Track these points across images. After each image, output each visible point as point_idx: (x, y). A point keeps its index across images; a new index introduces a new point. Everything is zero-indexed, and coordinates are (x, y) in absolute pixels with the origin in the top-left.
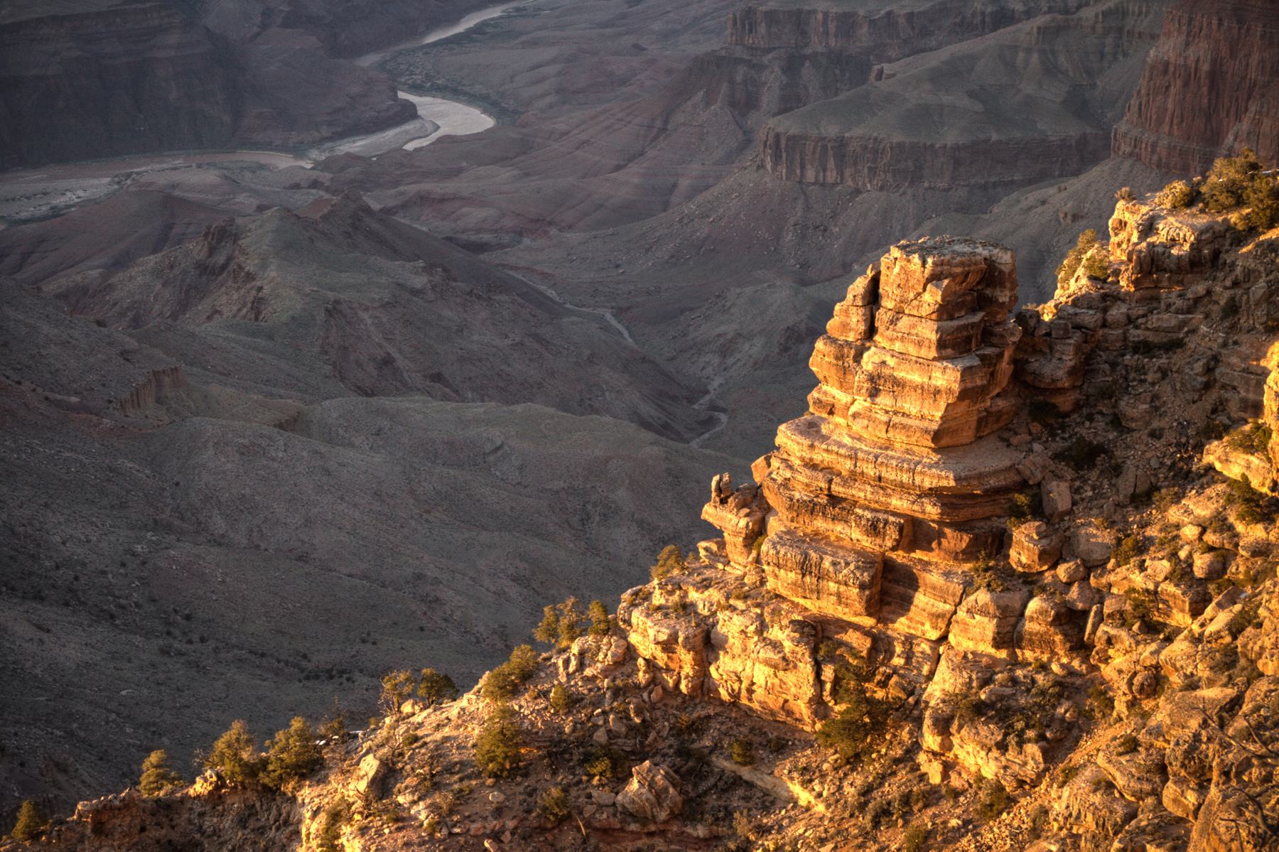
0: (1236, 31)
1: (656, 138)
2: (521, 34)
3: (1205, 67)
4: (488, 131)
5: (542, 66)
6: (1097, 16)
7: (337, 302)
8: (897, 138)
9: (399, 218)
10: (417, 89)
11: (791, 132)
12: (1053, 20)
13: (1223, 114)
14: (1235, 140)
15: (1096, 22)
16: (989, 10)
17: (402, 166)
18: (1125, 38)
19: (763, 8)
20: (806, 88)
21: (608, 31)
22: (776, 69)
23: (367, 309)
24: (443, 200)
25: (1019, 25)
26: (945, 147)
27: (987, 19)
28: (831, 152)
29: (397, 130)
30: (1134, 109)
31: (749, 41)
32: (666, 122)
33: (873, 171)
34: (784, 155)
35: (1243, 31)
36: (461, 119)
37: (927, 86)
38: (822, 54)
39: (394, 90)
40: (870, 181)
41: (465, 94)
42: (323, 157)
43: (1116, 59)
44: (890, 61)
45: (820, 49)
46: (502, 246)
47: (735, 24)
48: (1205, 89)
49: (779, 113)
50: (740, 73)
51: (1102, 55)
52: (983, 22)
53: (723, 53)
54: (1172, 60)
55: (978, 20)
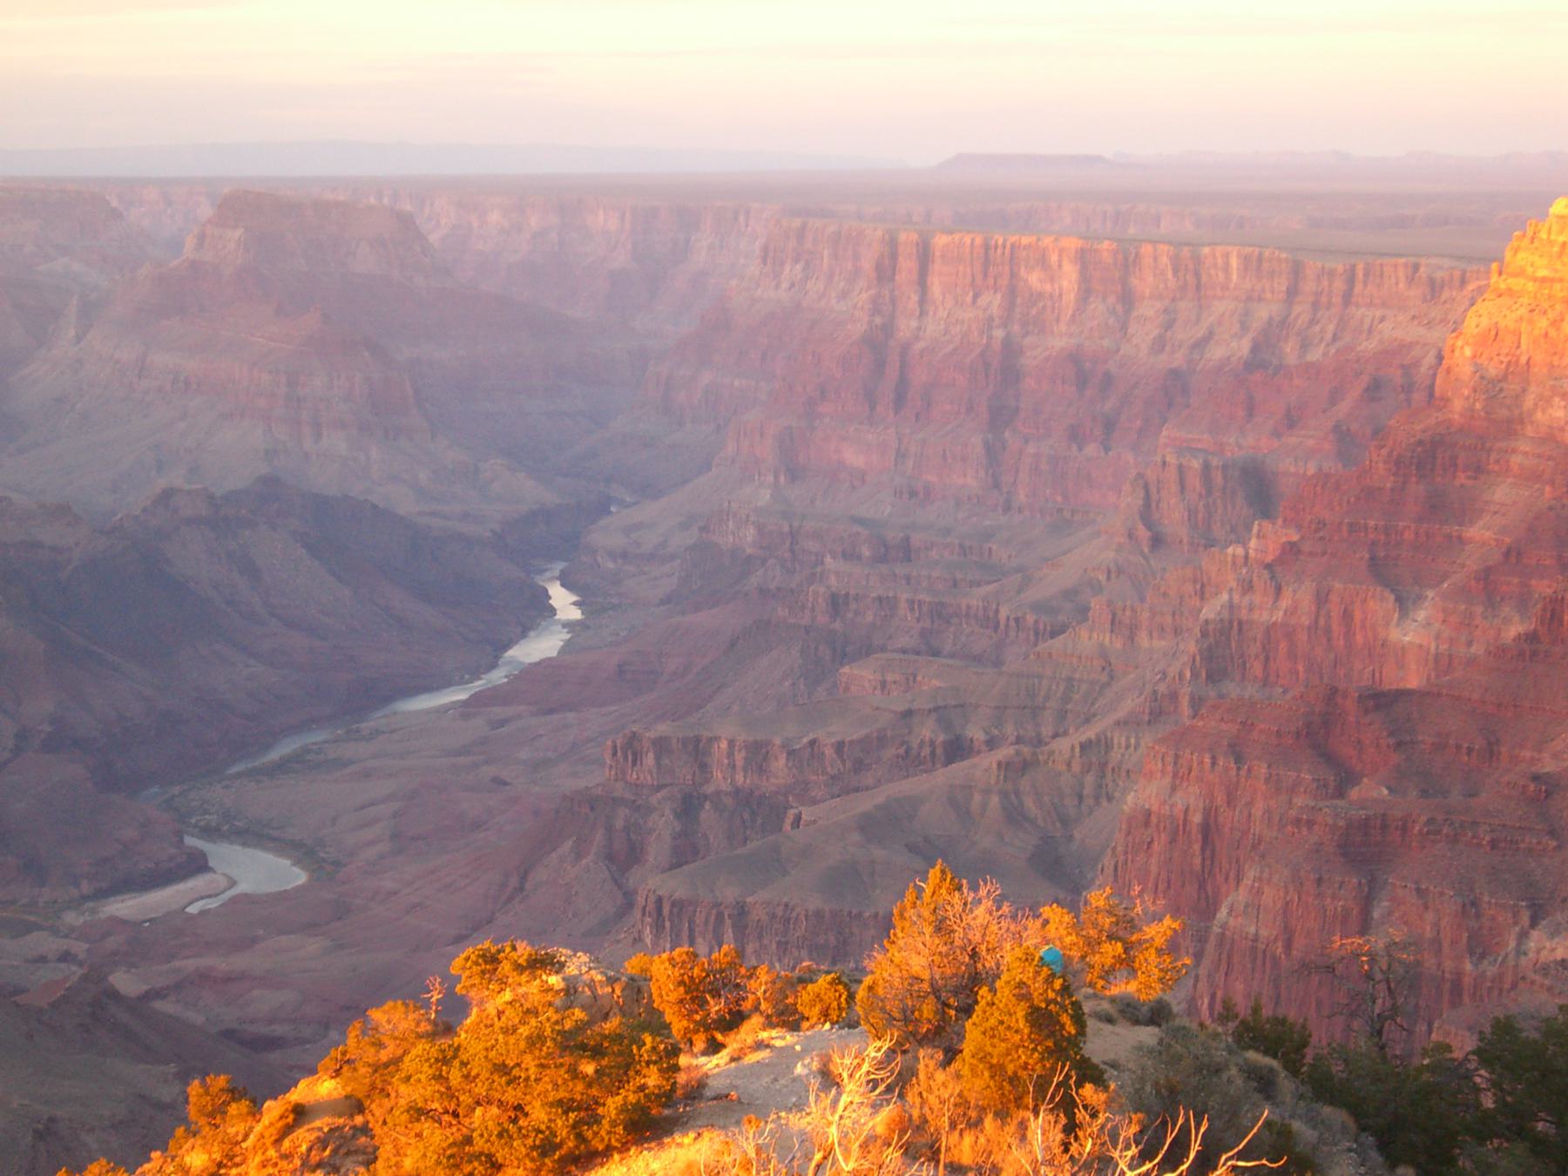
0: (1233, 773)
1: (510, 899)
2: (351, 762)
3: (1197, 819)
4: (298, 889)
5: (372, 804)
6: (1073, 748)
7: (52, 1120)
8: (815, 903)
9: (159, 1005)
10: (210, 833)
11: (677, 895)
12: (1018, 753)
13: (1220, 878)
14: (1229, 914)
15: (1073, 756)
16: (941, 738)
17: (178, 932)
18: (1109, 775)
19: (652, 734)
20: (705, 836)
21: (462, 760)
22: (667, 812)
23: (92, 1130)
24: (228, 979)
25: (975, 760)
26: (876, 916)
27: (939, 751)
28: (728, 922)
29: (181, 886)
30: (1109, 871)
31: (633, 776)
32: (524, 878)
33: (783, 947)
34: (668, 924)
35: (1243, 773)
36: (255, 872)
37: (856, 837)
38: (727, 794)
39: (179, 835)
40: (780, 960)
41: (274, 839)
42: (81, 920)
43: (1098, 803)
44: (814, 802)
45: (725, 787)
46: (301, 1041)
47: (615, 754)
48: (1197, 847)
49: (663, 872)
50: (620, 818)
51: (1080, 798)
52: (933, 753)
53: (599, 791)
54: (1155, 808)
55: (926, 751)
